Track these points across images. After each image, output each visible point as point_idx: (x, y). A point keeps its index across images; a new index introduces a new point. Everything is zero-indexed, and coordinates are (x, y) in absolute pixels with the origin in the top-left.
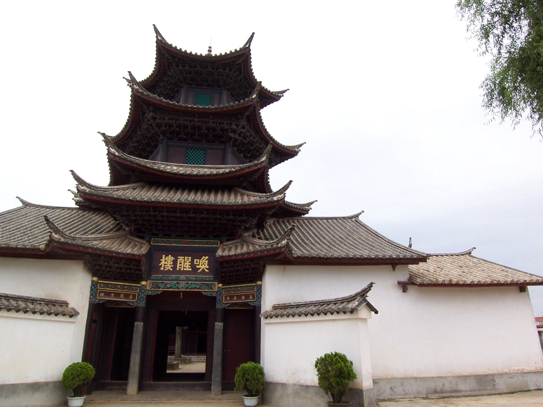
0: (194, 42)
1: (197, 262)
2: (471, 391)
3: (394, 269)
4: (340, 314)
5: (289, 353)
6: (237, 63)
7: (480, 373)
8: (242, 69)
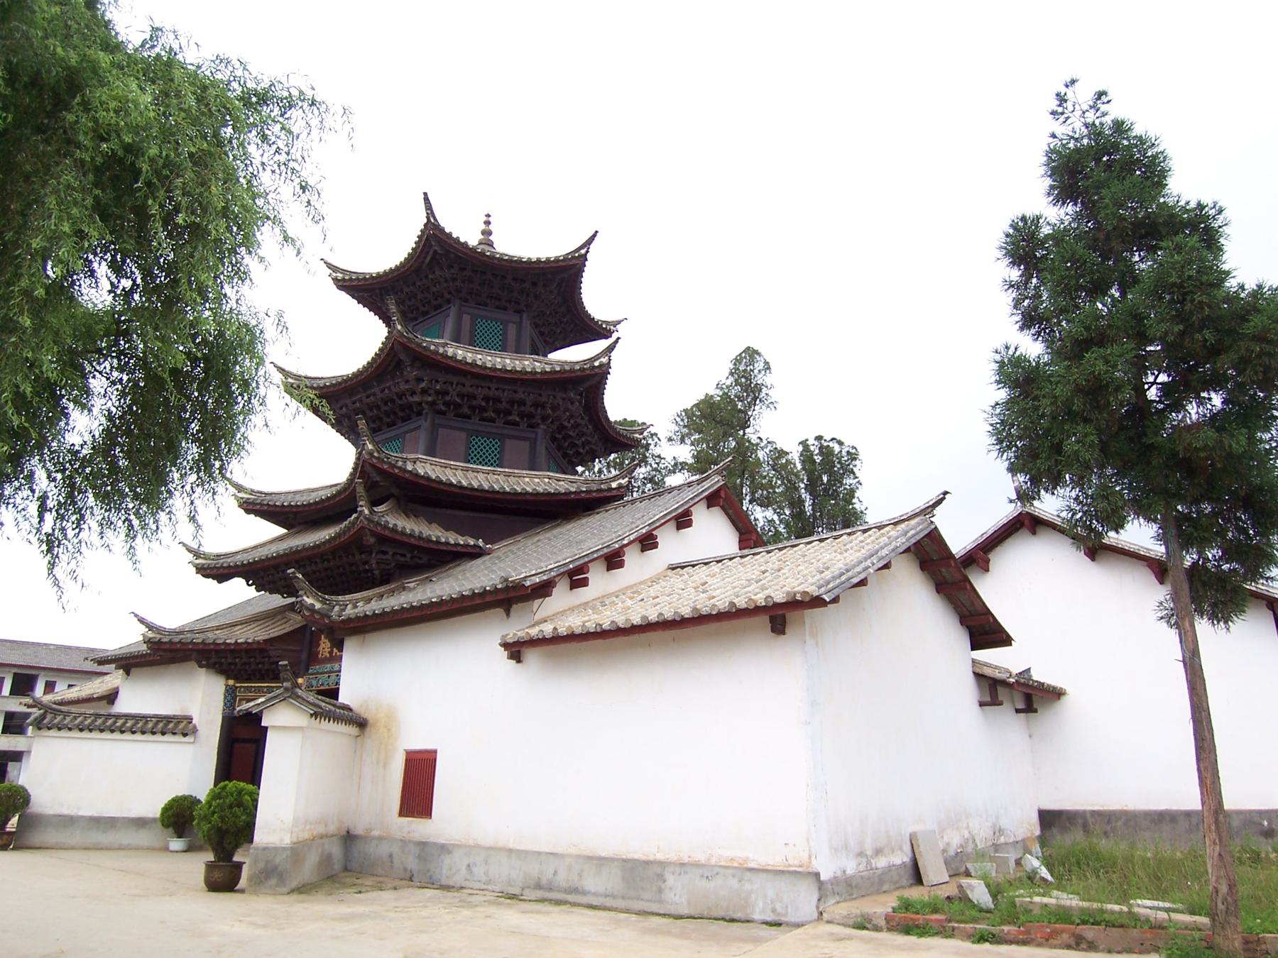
2: (606, 896)
3: (508, 615)
7: (636, 856)
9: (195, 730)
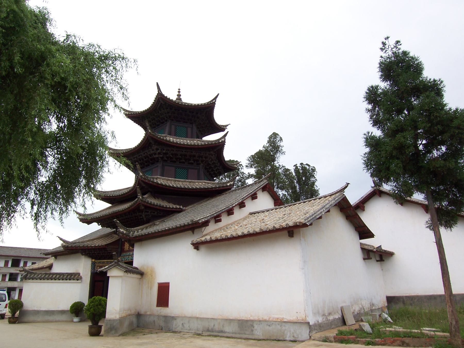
2: (233, 333)
3: (193, 233)
7: (243, 318)
9: (81, 278)
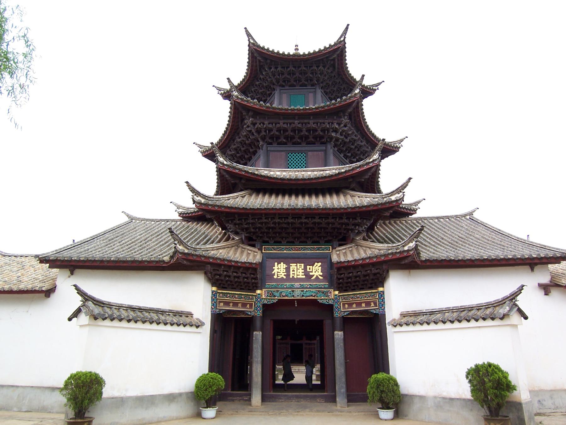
0: (284, 41)
1: (310, 269)
3: (532, 270)
4: (486, 321)
5: (427, 362)
6: (332, 58)
8: (336, 64)
